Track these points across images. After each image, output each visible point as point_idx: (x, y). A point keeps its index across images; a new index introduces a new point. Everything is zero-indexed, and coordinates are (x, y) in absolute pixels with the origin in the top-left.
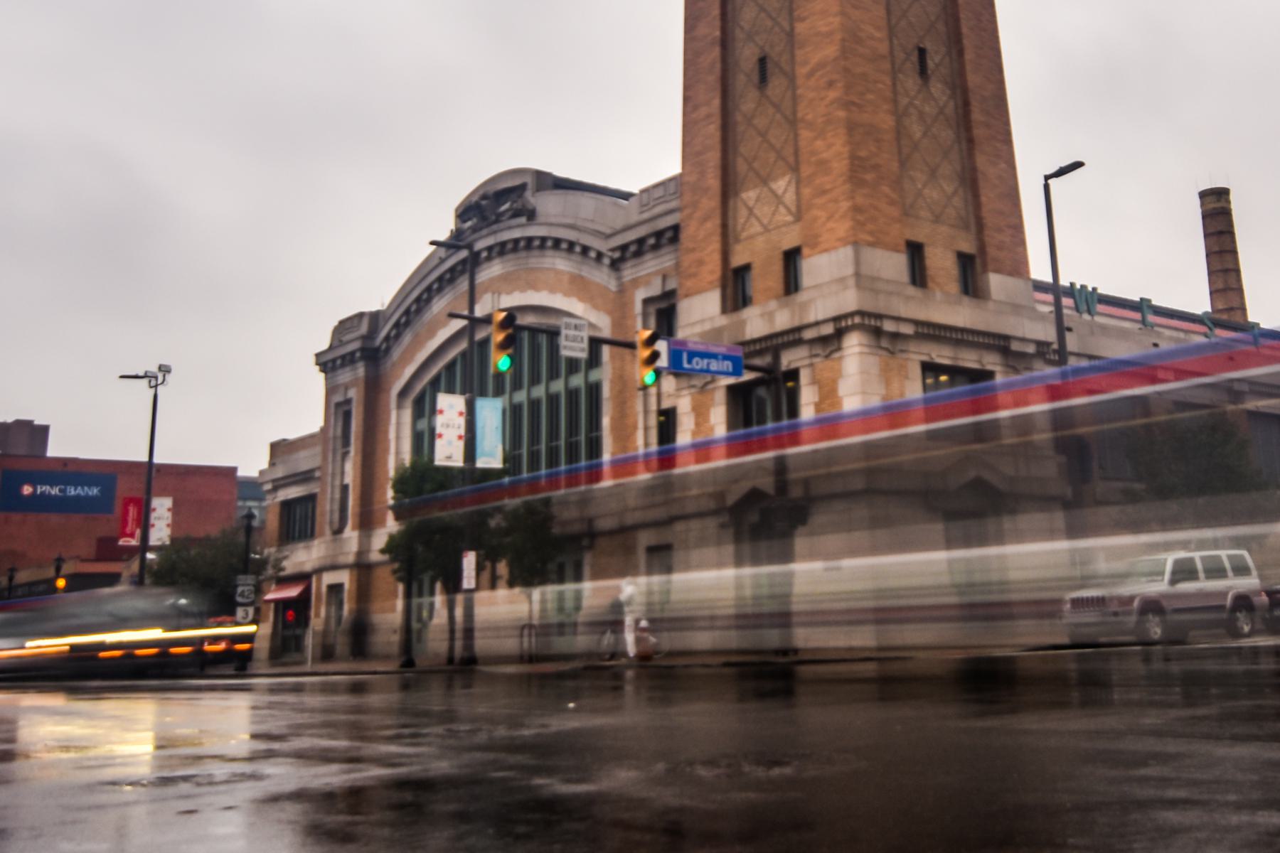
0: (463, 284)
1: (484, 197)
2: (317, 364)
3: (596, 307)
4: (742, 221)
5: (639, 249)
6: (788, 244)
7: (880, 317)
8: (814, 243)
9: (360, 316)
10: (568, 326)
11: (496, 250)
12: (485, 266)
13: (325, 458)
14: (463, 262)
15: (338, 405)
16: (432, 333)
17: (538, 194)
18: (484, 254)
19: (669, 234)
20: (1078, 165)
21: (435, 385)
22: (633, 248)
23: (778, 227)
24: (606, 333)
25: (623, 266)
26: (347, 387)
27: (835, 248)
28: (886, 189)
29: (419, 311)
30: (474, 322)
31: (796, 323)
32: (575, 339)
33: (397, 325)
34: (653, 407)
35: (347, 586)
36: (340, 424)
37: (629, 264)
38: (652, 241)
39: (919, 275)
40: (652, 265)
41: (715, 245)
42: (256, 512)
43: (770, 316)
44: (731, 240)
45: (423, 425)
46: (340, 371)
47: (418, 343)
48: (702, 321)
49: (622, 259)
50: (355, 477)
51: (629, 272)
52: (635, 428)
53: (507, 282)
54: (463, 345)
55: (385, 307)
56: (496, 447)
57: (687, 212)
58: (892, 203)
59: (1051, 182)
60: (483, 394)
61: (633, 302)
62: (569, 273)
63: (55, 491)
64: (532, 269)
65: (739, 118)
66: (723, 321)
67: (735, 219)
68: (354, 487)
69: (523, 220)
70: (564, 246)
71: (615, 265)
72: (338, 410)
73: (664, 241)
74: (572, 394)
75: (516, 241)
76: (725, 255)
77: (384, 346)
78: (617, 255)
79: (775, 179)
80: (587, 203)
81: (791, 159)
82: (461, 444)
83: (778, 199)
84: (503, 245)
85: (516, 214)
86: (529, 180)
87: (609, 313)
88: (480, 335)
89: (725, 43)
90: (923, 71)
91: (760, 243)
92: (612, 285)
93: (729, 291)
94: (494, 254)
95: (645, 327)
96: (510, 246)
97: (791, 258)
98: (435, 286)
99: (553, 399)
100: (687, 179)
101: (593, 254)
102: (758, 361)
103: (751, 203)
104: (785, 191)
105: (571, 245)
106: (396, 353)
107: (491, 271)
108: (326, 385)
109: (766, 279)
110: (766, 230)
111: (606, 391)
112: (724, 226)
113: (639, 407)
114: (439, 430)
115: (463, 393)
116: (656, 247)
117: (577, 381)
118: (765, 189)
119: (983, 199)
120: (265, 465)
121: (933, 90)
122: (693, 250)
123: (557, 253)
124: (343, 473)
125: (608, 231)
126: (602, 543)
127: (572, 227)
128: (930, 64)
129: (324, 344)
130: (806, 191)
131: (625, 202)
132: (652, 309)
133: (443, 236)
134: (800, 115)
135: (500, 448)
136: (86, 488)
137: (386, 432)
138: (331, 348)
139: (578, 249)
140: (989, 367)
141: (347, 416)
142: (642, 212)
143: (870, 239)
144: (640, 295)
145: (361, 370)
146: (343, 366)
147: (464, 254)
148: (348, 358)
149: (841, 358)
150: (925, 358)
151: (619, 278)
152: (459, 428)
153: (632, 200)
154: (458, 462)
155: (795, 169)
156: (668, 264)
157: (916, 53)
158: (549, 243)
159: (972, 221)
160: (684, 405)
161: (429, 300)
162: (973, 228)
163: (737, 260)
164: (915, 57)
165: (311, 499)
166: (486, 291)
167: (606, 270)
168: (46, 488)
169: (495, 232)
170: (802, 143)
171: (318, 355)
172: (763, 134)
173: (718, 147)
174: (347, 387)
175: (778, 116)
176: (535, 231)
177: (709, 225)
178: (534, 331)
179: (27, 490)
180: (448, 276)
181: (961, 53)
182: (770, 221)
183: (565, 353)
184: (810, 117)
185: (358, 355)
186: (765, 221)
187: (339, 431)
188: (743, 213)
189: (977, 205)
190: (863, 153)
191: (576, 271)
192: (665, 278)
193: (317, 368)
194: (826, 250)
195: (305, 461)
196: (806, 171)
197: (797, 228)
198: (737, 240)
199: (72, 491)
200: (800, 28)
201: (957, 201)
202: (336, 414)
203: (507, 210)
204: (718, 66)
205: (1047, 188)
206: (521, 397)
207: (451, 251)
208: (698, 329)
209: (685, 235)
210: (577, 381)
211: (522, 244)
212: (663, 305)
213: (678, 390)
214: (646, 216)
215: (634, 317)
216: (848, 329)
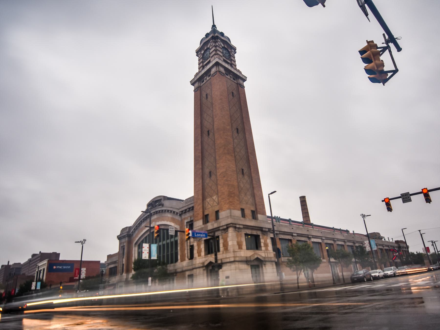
0: (148, 220)
1: (153, 202)
2: (117, 238)
3: (176, 224)
4: (206, 205)
5: (185, 212)
6: (216, 210)
7: (236, 224)
8: (222, 209)
9: (127, 227)
10: (170, 228)
11: (155, 213)
12: (153, 216)
13: (119, 258)
14: (148, 215)
15: (122, 247)
16: (142, 231)
17: (164, 201)
18: (153, 214)
19: (192, 208)
20: (275, 192)
21: (142, 242)
22: (184, 211)
23: (214, 206)
24: (179, 229)
25: (182, 215)
26: (124, 243)
27: (226, 210)
28: (236, 198)
29: (139, 226)
30: (151, 228)
31: (219, 226)
32: (172, 231)
33: (134, 229)
34: (189, 245)
37: (183, 215)
38: (188, 210)
39: (243, 215)
40: (188, 215)
41: (201, 210)
42: (104, 271)
43: (213, 225)
44: (204, 209)
45: (140, 250)
46: (122, 240)
47: (139, 233)
48: (199, 226)
49: (182, 214)
50: (125, 262)
51: (183, 217)
52: (185, 249)
53: (158, 219)
54: (148, 233)
55: (132, 225)
56: (155, 254)
57: (195, 203)
58: (237, 200)
59: (270, 195)
60: (153, 243)
61: (184, 223)
62: (171, 217)
63: (61, 267)
64: (162, 217)
65: (205, 184)
66: (203, 226)
67: (205, 204)
68: (125, 264)
69: (161, 206)
70: (170, 211)
71: (180, 215)
72: (122, 248)
73: (190, 210)
74: (172, 243)
75: (160, 211)
76: (203, 212)
77: (132, 234)
78: (181, 213)
79: (213, 196)
80: (174, 203)
81: (216, 192)
82: (148, 254)
83: (214, 200)
84: (157, 211)
85: (160, 205)
86: (162, 198)
87: (179, 225)
88: (152, 231)
89: (202, 169)
90: (243, 173)
91: (210, 209)
92: (180, 219)
93: (204, 220)
94: (155, 214)
95: (187, 228)
96: (158, 212)
97: (217, 212)
98: (143, 221)
99: (168, 244)
100: (195, 197)
101: (176, 213)
102: (210, 234)
103: (208, 201)
104: (215, 199)
105: (171, 211)
106: (134, 235)
107: (154, 217)
108: (119, 242)
109: (212, 217)
110: (212, 207)
111: (179, 242)
112: (203, 206)
113: (186, 245)
114: (143, 251)
115: (148, 243)
116: (189, 211)
117: (173, 240)
118: (211, 198)
119: (256, 199)
120: (106, 260)
121: (245, 177)
122: (197, 211)
123: (168, 213)
124: (123, 261)
125: (179, 208)
126: (178, 274)
127: (171, 207)
128: (244, 172)
129: (119, 234)
130: (220, 199)
131: (182, 202)
132: (188, 224)
133: (144, 210)
134: (218, 183)
135: (156, 255)
136: (67, 267)
137: (132, 252)
138: (120, 234)
139: (172, 212)
140: (259, 234)
141: (124, 249)
142: (186, 204)
143: (233, 208)
144: (186, 221)
145: (127, 239)
146: (123, 238)
147: (149, 214)
148: (124, 237)
149: (228, 233)
150: (245, 233)
151: (181, 218)
152: (147, 251)
153: (184, 201)
154: (147, 258)
155: (217, 194)
156: (192, 215)
157: (241, 170)
158: (167, 211)
159: (254, 203)
160: (195, 244)
161: (141, 224)
162: (254, 205)
163: (206, 213)
164: (241, 171)
165: (116, 267)
166: (153, 221)
167: (178, 216)
168: (59, 267)
169: (155, 209)
170: (219, 189)
171: (117, 236)
172: (211, 187)
173: (201, 190)
174: (124, 243)
175: (214, 183)
176: (163, 209)
177: (200, 206)
178: (163, 229)
179: (55, 267)
180: (145, 219)
181: (250, 170)
182: (212, 205)
183: (170, 234)
184: (220, 183)
185: (126, 236)
186: (211, 205)
187: (122, 252)
188: (207, 203)
189: (255, 201)
190: (231, 190)
191: (172, 217)
192: (191, 217)
193: (117, 239)
194: (224, 211)
195: (114, 259)
196: (219, 194)
197: (218, 206)
198: (206, 209)
199: (64, 267)
200: (218, 165)
201: (251, 200)
202: (121, 249)
203: (157, 205)
204: (201, 174)
205: (269, 196)
206: (161, 244)
207: (146, 213)
208: (198, 228)
209: (195, 208)
210: (173, 240)
211: (161, 211)
212: (191, 223)
213: (194, 241)
214: (187, 205)
215: (185, 226)
216: (230, 227)
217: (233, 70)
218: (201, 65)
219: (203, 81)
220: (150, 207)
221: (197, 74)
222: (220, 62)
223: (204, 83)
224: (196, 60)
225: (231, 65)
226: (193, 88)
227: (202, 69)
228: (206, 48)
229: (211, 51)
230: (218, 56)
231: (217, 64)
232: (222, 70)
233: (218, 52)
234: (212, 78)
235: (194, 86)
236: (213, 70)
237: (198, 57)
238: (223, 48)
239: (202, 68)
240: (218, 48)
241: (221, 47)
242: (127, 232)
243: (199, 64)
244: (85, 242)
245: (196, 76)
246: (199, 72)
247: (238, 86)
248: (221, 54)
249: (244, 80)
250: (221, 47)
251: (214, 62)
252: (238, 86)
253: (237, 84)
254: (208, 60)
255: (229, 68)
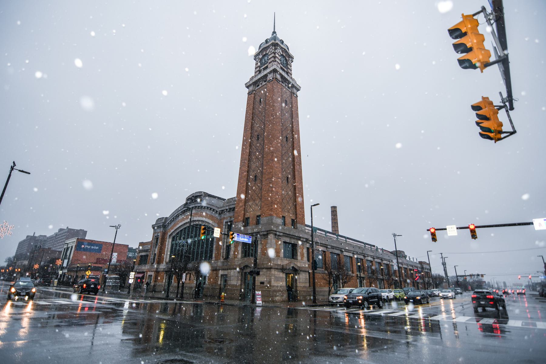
1: (193, 197)
15: (156, 236)
35: (153, 276)
36: (156, 240)
45: (174, 242)
47: (175, 225)
50: (158, 252)
72: (156, 238)
75: (199, 206)
84: (196, 207)
141: (157, 239)
165: (147, 256)
217: (289, 78)
218: (258, 69)
219: (259, 86)
220: (189, 202)
221: (253, 77)
222: (278, 69)
223: (259, 87)
224: (253, 64)
225: (287, 73)
226: (247, 91)
227: (259, 73)
228: (264, 53)
229: (269, 57)
230: (276, 63)
231: (275, 71)
232: (278, 77)
233: (277, 60)
234: (267, 83)
235: (248, 89)
236: (270, 77)
237: (256, 60)
238: (282, 55)
239: (258, 73)
240: (277, 55)
241: (280, 55)
242: (163, 223)
243: (256, 68)
244: (120, 227)
245: (251, 79)
246: (255, 76)
247: (292, 95)
248: (280, 62)
249: (298, 90)
250: (280, 55)
251: (272, 69)
252: (292, 95)
253: (291, 92)
254: (266, 65)
255: (286, 76)
